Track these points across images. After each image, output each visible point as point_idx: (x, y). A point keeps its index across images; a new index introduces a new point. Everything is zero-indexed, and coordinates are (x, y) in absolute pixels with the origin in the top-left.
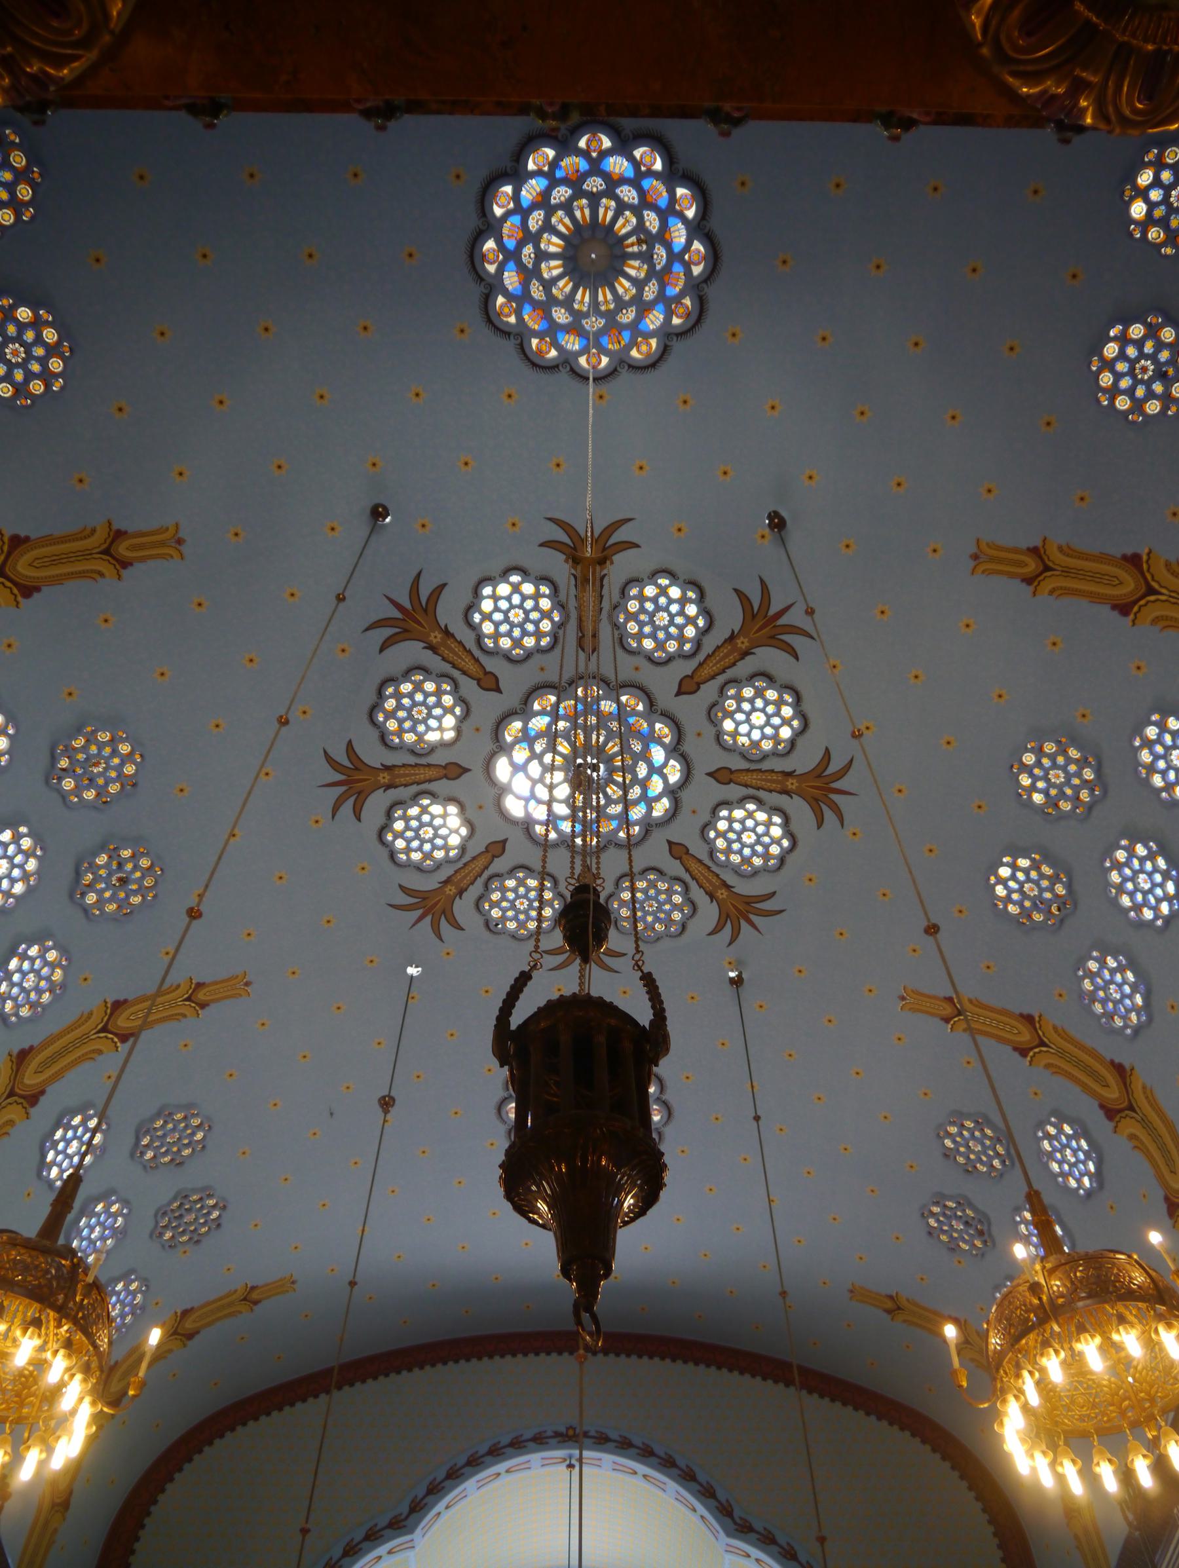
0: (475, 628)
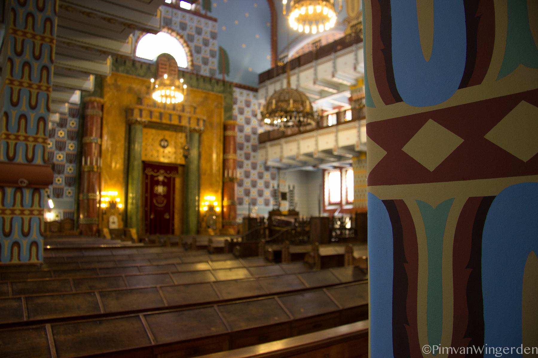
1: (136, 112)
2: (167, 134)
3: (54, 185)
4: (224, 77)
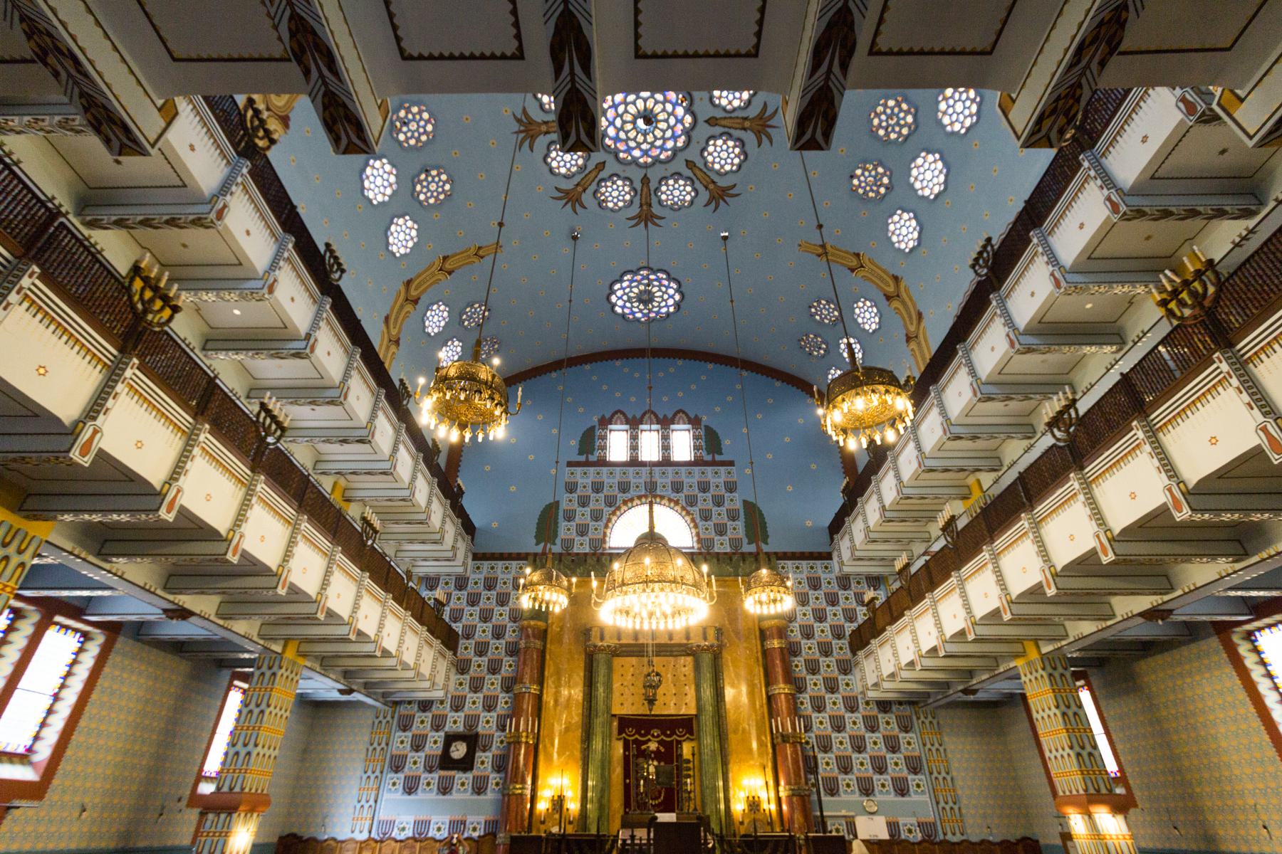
0: (695, 190)
3: (475, 772)
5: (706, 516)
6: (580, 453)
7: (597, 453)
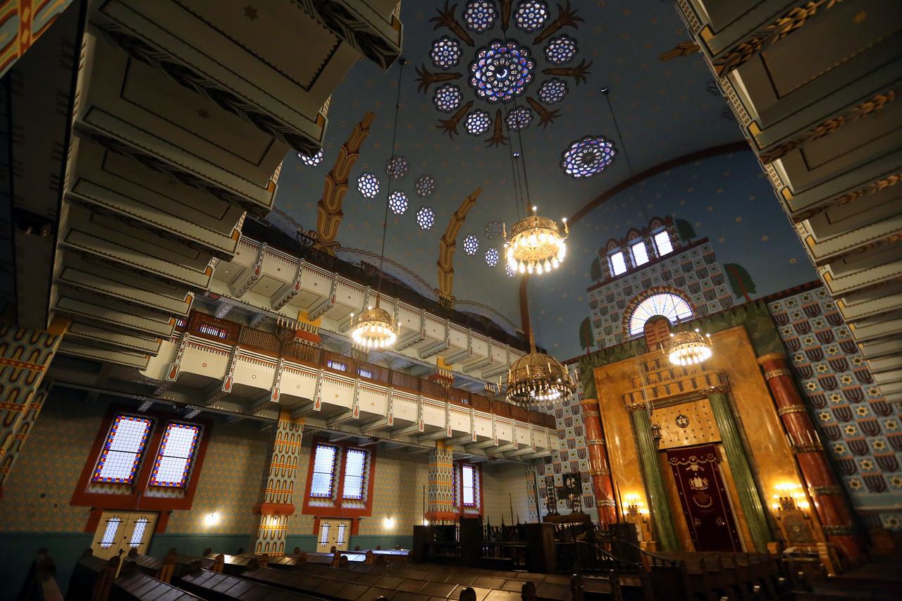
1: (627, 398)
2: (682, 408)
4: (747, 298)
5: (695, 289)
6: (593, 280)
7: (604, 275)
